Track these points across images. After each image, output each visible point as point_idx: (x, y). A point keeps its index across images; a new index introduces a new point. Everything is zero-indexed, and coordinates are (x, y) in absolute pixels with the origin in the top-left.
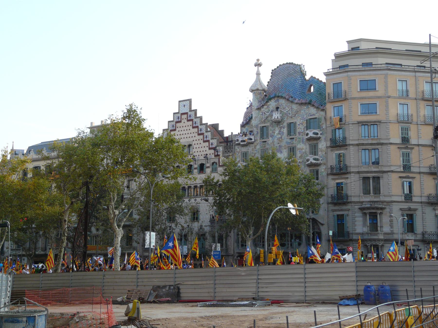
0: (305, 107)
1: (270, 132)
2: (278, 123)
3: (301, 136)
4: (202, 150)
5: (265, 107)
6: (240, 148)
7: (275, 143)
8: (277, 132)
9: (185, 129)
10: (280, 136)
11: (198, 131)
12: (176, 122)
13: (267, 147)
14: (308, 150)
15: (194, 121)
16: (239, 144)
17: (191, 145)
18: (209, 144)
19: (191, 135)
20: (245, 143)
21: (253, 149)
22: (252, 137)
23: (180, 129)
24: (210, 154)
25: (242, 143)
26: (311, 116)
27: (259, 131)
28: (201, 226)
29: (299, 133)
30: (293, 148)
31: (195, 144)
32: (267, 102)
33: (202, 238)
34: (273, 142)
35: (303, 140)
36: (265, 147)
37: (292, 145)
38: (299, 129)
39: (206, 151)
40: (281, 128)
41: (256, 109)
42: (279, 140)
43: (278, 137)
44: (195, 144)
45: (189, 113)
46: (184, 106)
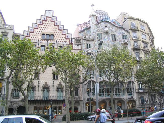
0: (120, 29)
1: (103, 37)
2: (107, 33)
4: (61, 38)
9: (49, 25)
11: (58, 28)
15: (55, 22)
16: (86, 40)
17: (53, 35)
18: (66, 36)
19: (53, 30)
23: (46, 25)
24: (66, 42)
29: (118, 40)
31: (56, 35)
32: (101, 22)
39: (63, 39)
43: (107, 40)
44: (56, 35)
45: (52, 18)
46: (49, 13)
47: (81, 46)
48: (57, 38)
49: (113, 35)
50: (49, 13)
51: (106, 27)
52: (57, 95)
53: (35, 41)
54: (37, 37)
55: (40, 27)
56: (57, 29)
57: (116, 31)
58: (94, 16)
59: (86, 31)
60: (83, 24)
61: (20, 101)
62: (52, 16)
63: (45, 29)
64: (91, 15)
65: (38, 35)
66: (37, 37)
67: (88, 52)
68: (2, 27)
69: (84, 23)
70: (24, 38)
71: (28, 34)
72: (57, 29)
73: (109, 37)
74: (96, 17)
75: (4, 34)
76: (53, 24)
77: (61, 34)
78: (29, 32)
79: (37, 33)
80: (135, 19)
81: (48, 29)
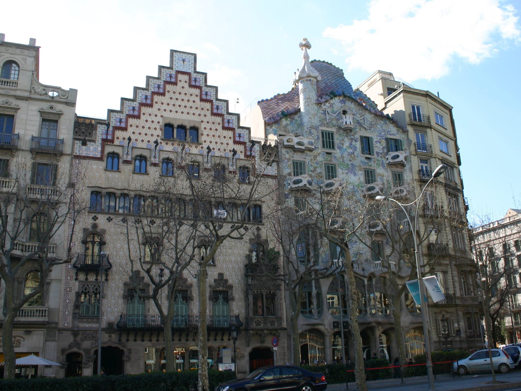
0: (382, 122)
1: (337, 142)
2: (348, 131)
3: (379, 158)
5: (327, 104)
6: (291, 154)
7: (345, 159)
8: (347, 144)
9: (186, 98)
10: (350, 151)
11: (212, 108)
12: (164, 81)
13: (334, 161)
14: (390, 178)
15: (203, 89)
18: (234, 134)
19: (197, 112)
20: (303, 148)
21: (311, 160)
22: (313, 141)
25: (296, 146)
26: (390, 135)
27: (320, 136)
28: (221, 275)
29: (378, 153)
30: (371, 172)
31: (205, 128)
32: (332, 98)
33: (221, 297)
34: (342, 157)
35: (383, 164)
36: (330, 160)
37: (370, 168)
38: (377, 148)
40: (352, 140)
41: (316, 103)
42: (351, 156)
45: (194, 75)
46: (184, 61)
47: (278, 165)
48: (208, 139)
49: (365, 137)
50: (184, 61)
51: (345, 112)
52: (212, 312)
53: (144, 145)
54: (149, 132)
55: (156, 103)
56: (208, 110)
57: (371, 126)
58: (312, 79)
59: (284, 122)
60: (272, 99)
61: (103, 330)
62: (193, 70)
63: (174, 109)
64: (305, 75)
65: (153, 126)
66: (149, 132)
67: (300, 185)
68: (41, 95)
69: (275, 97)
70: (110, 132)
71: (121, 121)
72: (210, 112)
73: (354, 143)
74: (318, 81)
75: (47, 117)
76: (197, 96)
77: (220, 127)
78: (125, 115)
79: (150, 119)
80: (423, 95)
81: (182, 109)
